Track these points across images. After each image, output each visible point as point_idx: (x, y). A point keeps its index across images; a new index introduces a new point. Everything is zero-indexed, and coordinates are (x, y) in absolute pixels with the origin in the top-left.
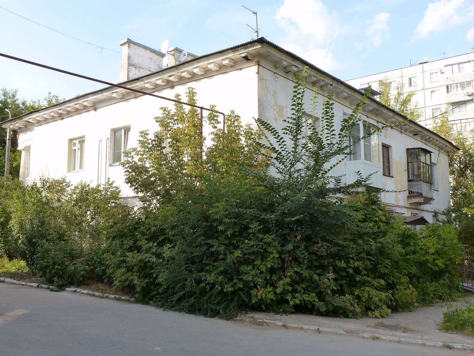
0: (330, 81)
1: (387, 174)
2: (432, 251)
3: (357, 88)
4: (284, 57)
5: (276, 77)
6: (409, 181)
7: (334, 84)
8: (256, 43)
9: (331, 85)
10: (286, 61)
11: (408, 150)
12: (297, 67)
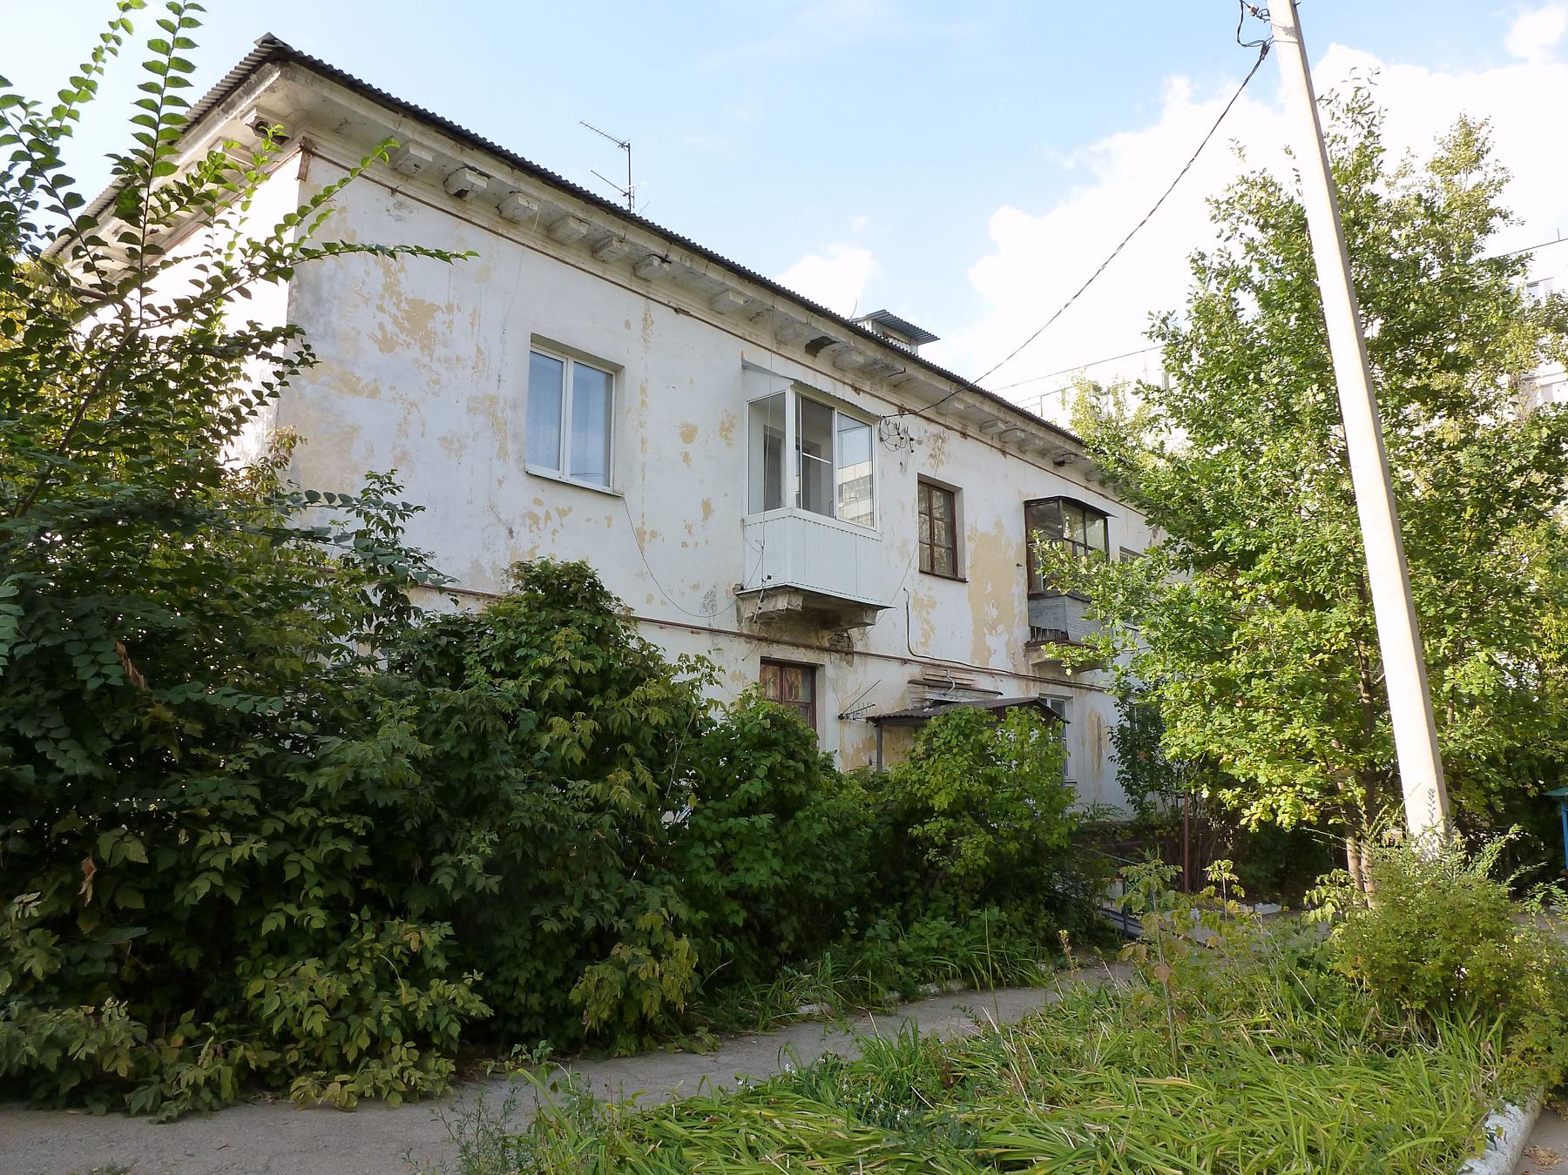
0: (656, 247)
1: (943, 566)
2: (941, 802)
3: (846, 314)
4: (410, 130)
5: (400, 205)
6: (1031, 597)
7: (672, 257)
8: (268, 65)
9: (664, 260)
10: (426, 149)
11: (1028, 504)
12: (488, 177)
